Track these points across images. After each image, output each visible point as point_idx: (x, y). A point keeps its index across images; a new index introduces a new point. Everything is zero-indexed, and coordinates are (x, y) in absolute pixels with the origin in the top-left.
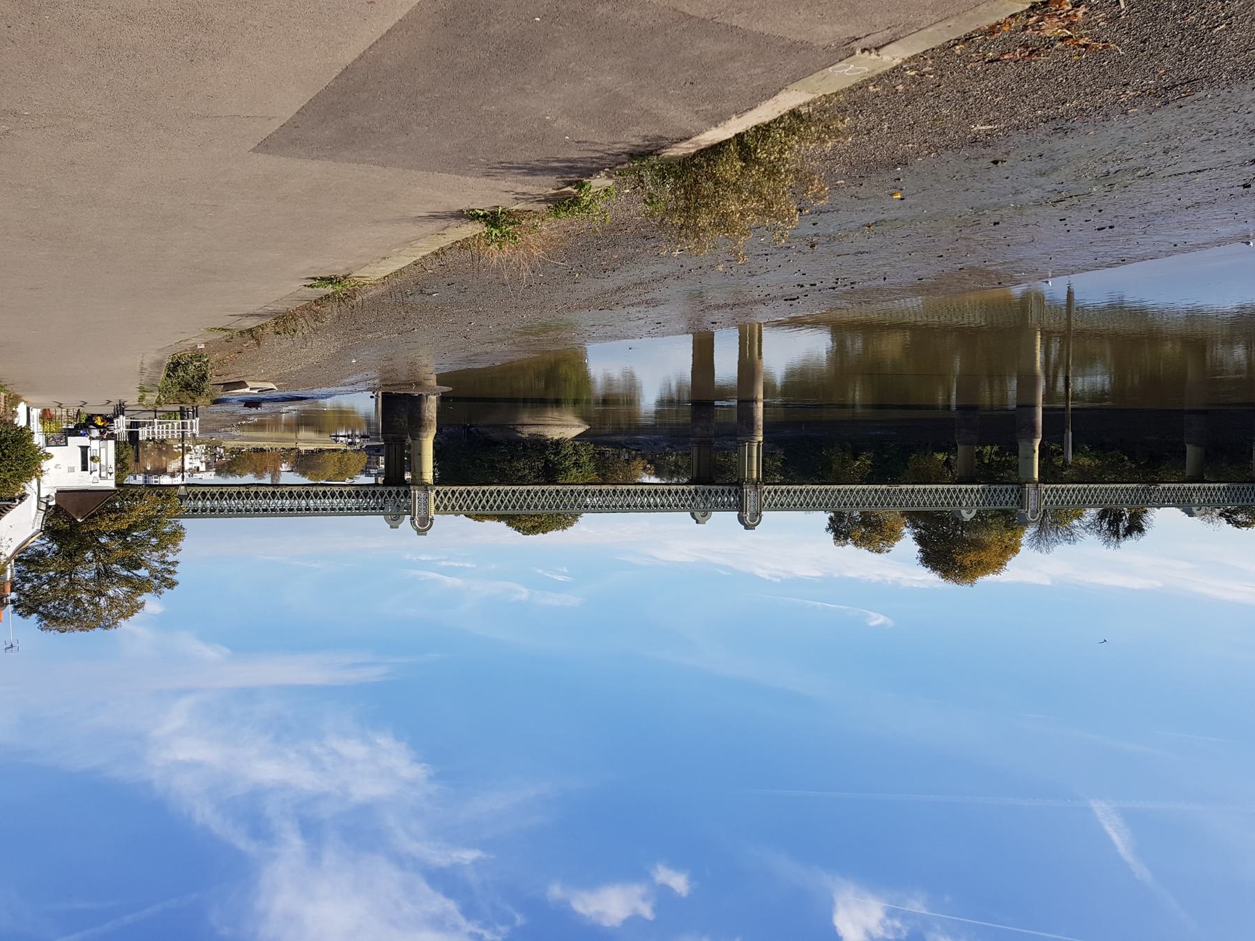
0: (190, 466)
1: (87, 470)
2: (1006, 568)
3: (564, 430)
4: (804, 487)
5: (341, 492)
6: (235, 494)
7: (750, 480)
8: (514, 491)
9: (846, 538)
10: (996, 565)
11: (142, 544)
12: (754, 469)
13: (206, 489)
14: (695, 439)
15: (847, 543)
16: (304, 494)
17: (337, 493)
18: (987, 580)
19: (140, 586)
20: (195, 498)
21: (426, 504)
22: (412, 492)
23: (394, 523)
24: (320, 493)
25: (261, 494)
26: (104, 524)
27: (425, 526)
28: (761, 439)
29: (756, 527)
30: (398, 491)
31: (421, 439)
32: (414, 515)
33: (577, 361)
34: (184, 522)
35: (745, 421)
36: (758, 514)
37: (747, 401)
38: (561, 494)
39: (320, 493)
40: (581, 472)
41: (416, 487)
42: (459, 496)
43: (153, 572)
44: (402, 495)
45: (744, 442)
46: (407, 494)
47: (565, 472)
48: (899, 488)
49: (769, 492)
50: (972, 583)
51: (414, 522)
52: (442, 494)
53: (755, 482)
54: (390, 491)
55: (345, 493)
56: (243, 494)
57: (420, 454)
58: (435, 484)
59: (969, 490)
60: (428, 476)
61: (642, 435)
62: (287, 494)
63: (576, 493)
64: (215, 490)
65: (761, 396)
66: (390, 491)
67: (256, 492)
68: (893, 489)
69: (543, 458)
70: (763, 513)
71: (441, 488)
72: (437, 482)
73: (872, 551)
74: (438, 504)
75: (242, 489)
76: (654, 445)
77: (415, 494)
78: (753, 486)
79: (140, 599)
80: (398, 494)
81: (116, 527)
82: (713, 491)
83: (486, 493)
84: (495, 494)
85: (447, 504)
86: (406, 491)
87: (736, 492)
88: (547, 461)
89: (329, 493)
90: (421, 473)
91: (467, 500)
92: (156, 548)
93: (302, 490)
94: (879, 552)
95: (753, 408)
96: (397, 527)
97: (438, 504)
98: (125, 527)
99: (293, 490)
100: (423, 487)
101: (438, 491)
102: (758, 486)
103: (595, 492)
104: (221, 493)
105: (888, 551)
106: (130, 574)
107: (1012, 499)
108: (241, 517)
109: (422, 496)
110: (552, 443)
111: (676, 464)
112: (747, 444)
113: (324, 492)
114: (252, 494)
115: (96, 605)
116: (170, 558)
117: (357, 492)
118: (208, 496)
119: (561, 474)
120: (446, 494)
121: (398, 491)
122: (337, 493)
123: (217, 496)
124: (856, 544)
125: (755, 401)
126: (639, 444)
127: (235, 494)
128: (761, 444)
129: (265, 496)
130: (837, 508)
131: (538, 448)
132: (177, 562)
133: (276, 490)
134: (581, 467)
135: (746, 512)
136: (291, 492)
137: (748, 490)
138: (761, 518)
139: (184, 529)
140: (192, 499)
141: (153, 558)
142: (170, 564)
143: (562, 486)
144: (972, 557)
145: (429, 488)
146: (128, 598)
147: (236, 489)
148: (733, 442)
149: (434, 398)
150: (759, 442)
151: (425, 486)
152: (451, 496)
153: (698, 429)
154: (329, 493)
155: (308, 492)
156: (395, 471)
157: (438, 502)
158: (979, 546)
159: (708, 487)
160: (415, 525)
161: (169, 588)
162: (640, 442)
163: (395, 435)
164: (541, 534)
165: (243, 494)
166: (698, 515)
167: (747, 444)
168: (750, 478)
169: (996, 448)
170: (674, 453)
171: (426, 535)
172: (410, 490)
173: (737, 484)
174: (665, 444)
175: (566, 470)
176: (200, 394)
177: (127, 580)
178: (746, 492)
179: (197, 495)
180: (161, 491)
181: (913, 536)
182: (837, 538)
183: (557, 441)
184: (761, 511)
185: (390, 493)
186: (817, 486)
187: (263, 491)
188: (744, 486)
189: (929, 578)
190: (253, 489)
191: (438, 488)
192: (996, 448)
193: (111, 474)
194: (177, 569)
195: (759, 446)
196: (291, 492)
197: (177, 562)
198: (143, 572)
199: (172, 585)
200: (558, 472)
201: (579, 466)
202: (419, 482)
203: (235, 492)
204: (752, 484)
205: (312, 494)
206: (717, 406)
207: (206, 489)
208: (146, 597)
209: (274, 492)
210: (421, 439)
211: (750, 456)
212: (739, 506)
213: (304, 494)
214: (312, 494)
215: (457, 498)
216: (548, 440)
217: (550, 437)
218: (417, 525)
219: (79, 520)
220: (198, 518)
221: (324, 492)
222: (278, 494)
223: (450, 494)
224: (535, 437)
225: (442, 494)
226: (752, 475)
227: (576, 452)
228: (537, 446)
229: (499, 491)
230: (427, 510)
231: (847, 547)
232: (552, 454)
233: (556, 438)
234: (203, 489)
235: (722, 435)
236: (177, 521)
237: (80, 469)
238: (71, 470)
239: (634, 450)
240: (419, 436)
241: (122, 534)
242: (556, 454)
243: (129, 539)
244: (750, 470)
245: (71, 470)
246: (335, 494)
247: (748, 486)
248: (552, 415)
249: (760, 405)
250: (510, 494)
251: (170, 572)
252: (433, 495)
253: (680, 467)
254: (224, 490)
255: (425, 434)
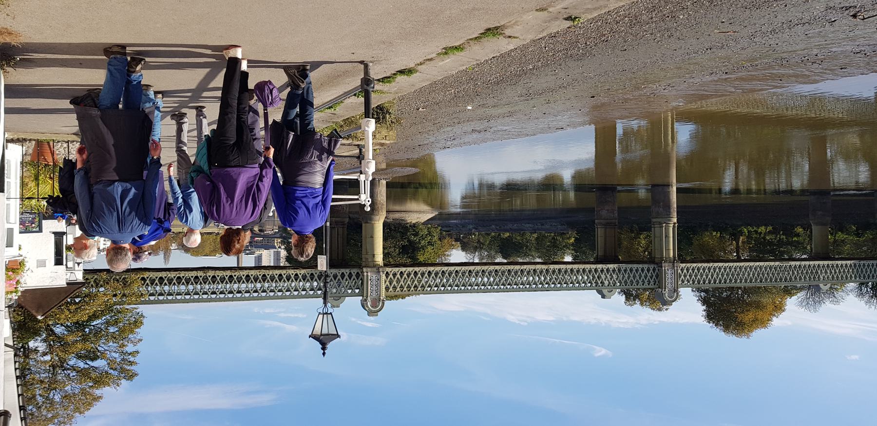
0: (104, 246)
1: (62, 264)
2: (772, 323)
3: (420, 215)
4: (711, 264)
5: (296, 275)
6: (192, 279)
7: (668, 260)
8: (457, 271)
9: (634, 300)
10: (763, 323)
11: (97, 333)
12: (671, 249)
13: (163, 274)
14: (602, 221)
15: (635, 303)
16: (260, 277)
17: (293, 276)
18: (758, 334)
19: (101, 380)
20: (152, 284)
21: (378, 286)
22: (365, 274)
23: (335, 303)
24: (276, 277)
25: (218, 278)
26: (63, 316)
27: (376, 307)
28: (675, 220)
29: (673, 303)
30: (350, 273)
31: (373, 222)
32: (367, 297)
33: (428, 162)
34: (142, 309)
35: (661, 204)
36: (676, 290)
37: (664, 185)
38: (500, 273)
39: (276, 277)
40: (433, 249)
41: (369, 269)
42: (407, 277)
43: (111, 363)
44: (354, 277)
45: (661, 223)
46: (358, 275)
47: (423, 249)
48: (789, 264)
49: (682, 270)
50: (748, 338)
51: (367, 304)
52: (391, 276)
53: (672, 260)
54: (343, 273)
55: (300, 276)
56: (201, 279)
57: (372, 237)
58: (385, 265)
59: (844, 265)
60: (379, 259)
61: (454, 220)
62: (244, 278)
63: (513, 273)
64: (172, 275)
65: (674, 181)
66: (343, 273)
67: (214, 277)
68: (784, 266)
69: (405, 239)
70: (679, 290)
71: (390, 269)
72: (385, 265)
73: (654, 309)
74: (387, 285)
75: (200, 274)
76: (463, 227)
77: (368, 275)
78: (671, 264)
79: (97, 392)
80: (343, 275)
81: (75, 319)
82: (634, 269)
83: (417, 274)
84: (440, 275)
85: (396, 285)
86: (358, 273)
87: (654, 270)
88: (409, 241)
89: (284, 276)
90: (374, 256)
91: (407, 281)
92: (114, 337)
93: (258, 274)
94: (660, 310)
95: (669, 192)
96: (338, 307)
97: (387, 285)
98: (85, 318)
99: (250, 274)
100: (375, 269)
101: (387, 273)
102: (675, 264)
103: (530, 271)
104: (179, 278)
105: (667, 309)
106: (87, 366)
107: (868, 273)
108: (199, 302)
109: (374, 278)
110: (410, 226)
111: (479, 241)
112: (664, 225)
113: (280, 275)
114: (210, 279)
115: (52, 403)
116: (130, 348)
117: (312, 274)
118: (166, 281)
119: (420, 251)
120: (395, 275)
121: (350, 273)
122: (293, 276)
123: (175, 281)
124: (642, 304)
125: (668, 185)
126: (450, 227)
127: (192, 279)
128: (676, 225)
129: (222, 280)
130: (734, 284)
131: (400, 230)
132: (138, 352)
133: (233, 274)
134: (433, 245)
135: (665, 288)
136: (248, 276)
137: (666, 266)
138: (678, 294)
139: (144, 317)
140: (150, 284)
141: (109, 347)
142: (130, 354)
143: (501, 266)
144: (750, 316)
145: (381, 270)
146: (84, 392)
147: (194, 274)
148: (530, 225)
149: (384, 182)
150: (675, 223)
151: (377, 268)
152: (399, 277)
153: (604, 213)
154: (284, 276)
155: (264, 275)
156: (338, 254)
157: (388, 283)
158: (759, 306)
159: (630, 266)
160: (368, 307)
161: (128, 379)
162: (451, 225)
163: (337, 219)
164: (401, 299)
165: (201, 279)
166: (605, 291)
167: (664, 225)
168: (667, 257)
169: (770, 228)
170: (477, 233)
171: (377, 315)
172: (362, 272)
173: (651, 261)
174: (471, 227)
175: (423, 248)
176: (384, 118)
177: (84, 374)
178: (665, 270)
179: (154, 280)
180: (118, 277)
181: (697, 298)
182: (627, 299)
183: (414, 224)
184: (678, 288)
185: (343, 275)
186: (723, 264)
187: (220, 275)
188: (663, 265)
189: (716, 333)
190: (211, 273)
191: (388, 270)
192: (770, 228)
193: (79, 264)
194: (137, 359)
195: (674, 227)
196: (248, 276)
197: (138, 352)
198: (100, 363)
199: (130, 376)
200: (418, 249)
201: (431, 245)
202: (371, 264)
203: (192, 277)
204: (670, 262)
205: (268, 277)
206: (619, 191)
207: (163, 274)
208: (106, 391)
209: (231, 276)
210: (373, 222)
211: (667, 236)
212: (657, 283)
213: (260, 277)
214: (268, 277)
215: (405, 278)
216: (407, 224)
217: (408, 221)
218: (370, 307)
219: (39, 318)
220: (155, 304)
221: (280, 275)
222: (235, 278)
223: (398, 276)
224: (398, 222)
225: (391, 276)
226: (669, 254)
227: (430, 233)
228: (399, 229)
229: (443, 271)
230: (378, 291)
231: (635, 305)
232: (413, 235)
233: (414, 222)
234: (160, 274)
235: (523, 220)
236: (136, 309)
237: (54, 264)
238: (42, 264)
239: (444, 231)
240: (371, 219)
241: (79, 326)
242: (416, 235)
243: (87, 330)
244: (668, 250)
245: (42, 264)
246: (291, 277)
247: (667, 264)
248: (412, 205)
249: (675, 189)
250: (454, 274)
251: (131, 363)
252: (384, 277)
253: (482, 244)
254: (182, 274)
255: (377, 217)
